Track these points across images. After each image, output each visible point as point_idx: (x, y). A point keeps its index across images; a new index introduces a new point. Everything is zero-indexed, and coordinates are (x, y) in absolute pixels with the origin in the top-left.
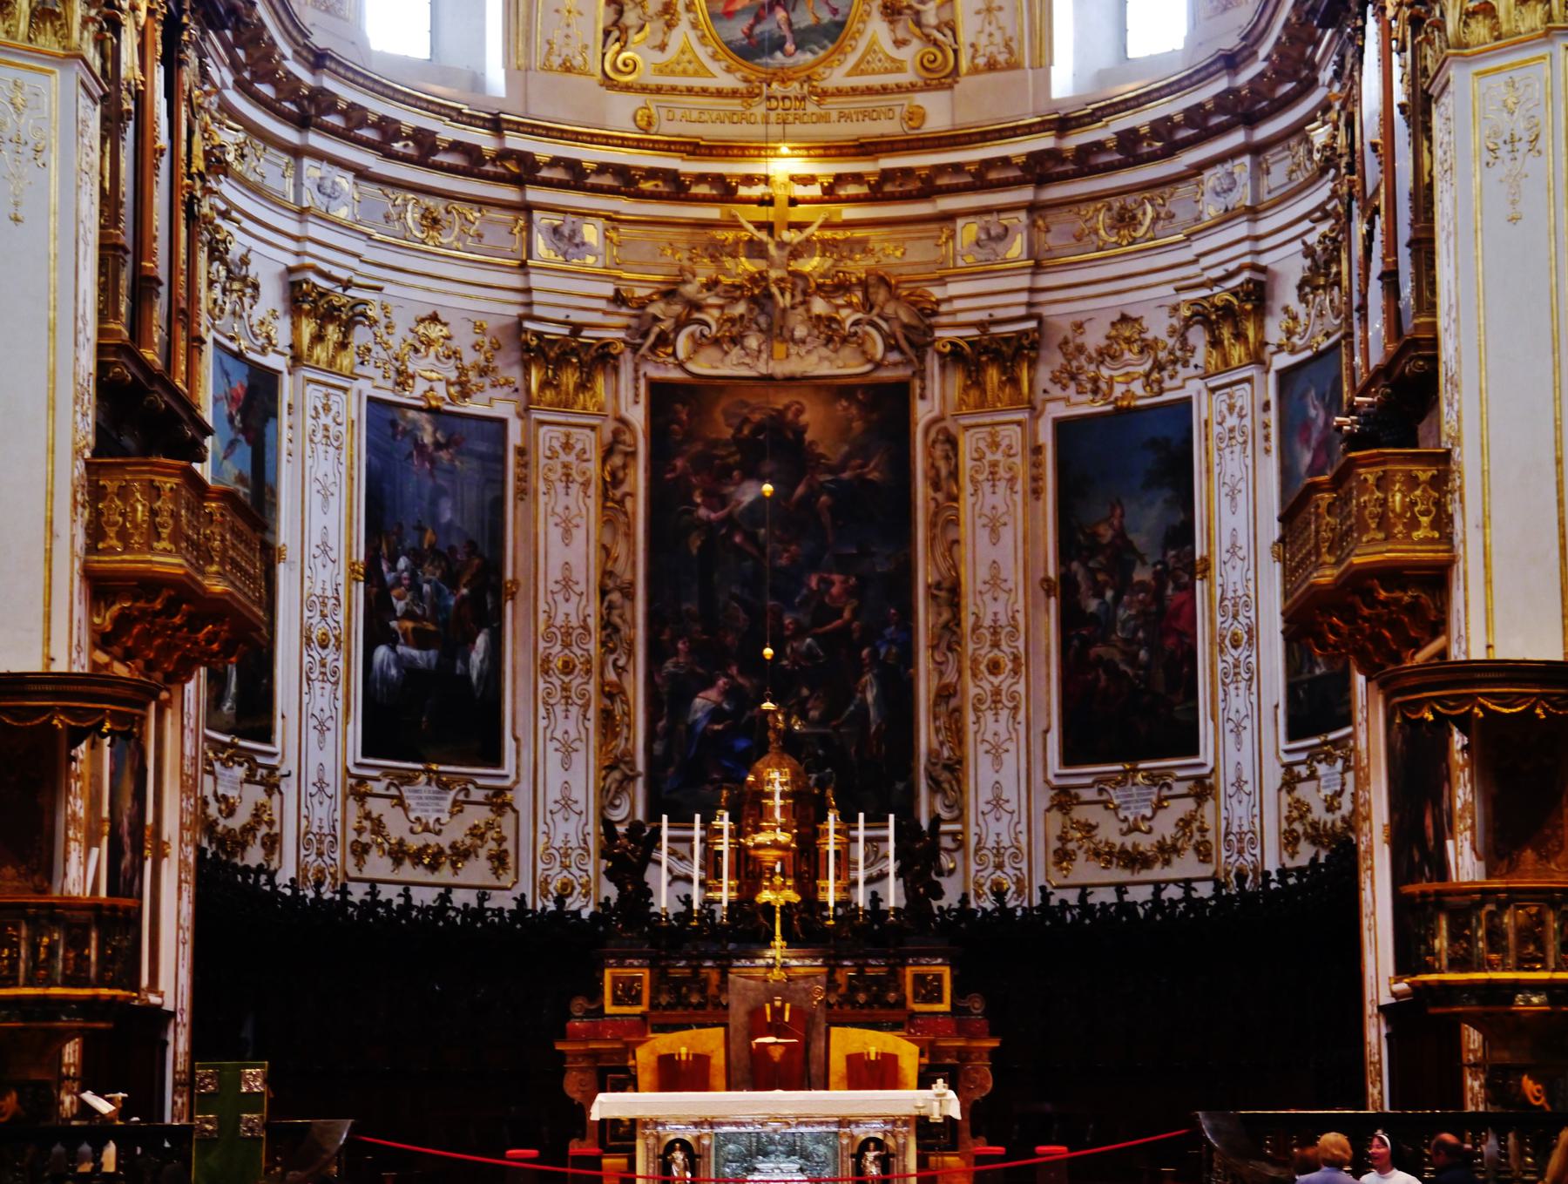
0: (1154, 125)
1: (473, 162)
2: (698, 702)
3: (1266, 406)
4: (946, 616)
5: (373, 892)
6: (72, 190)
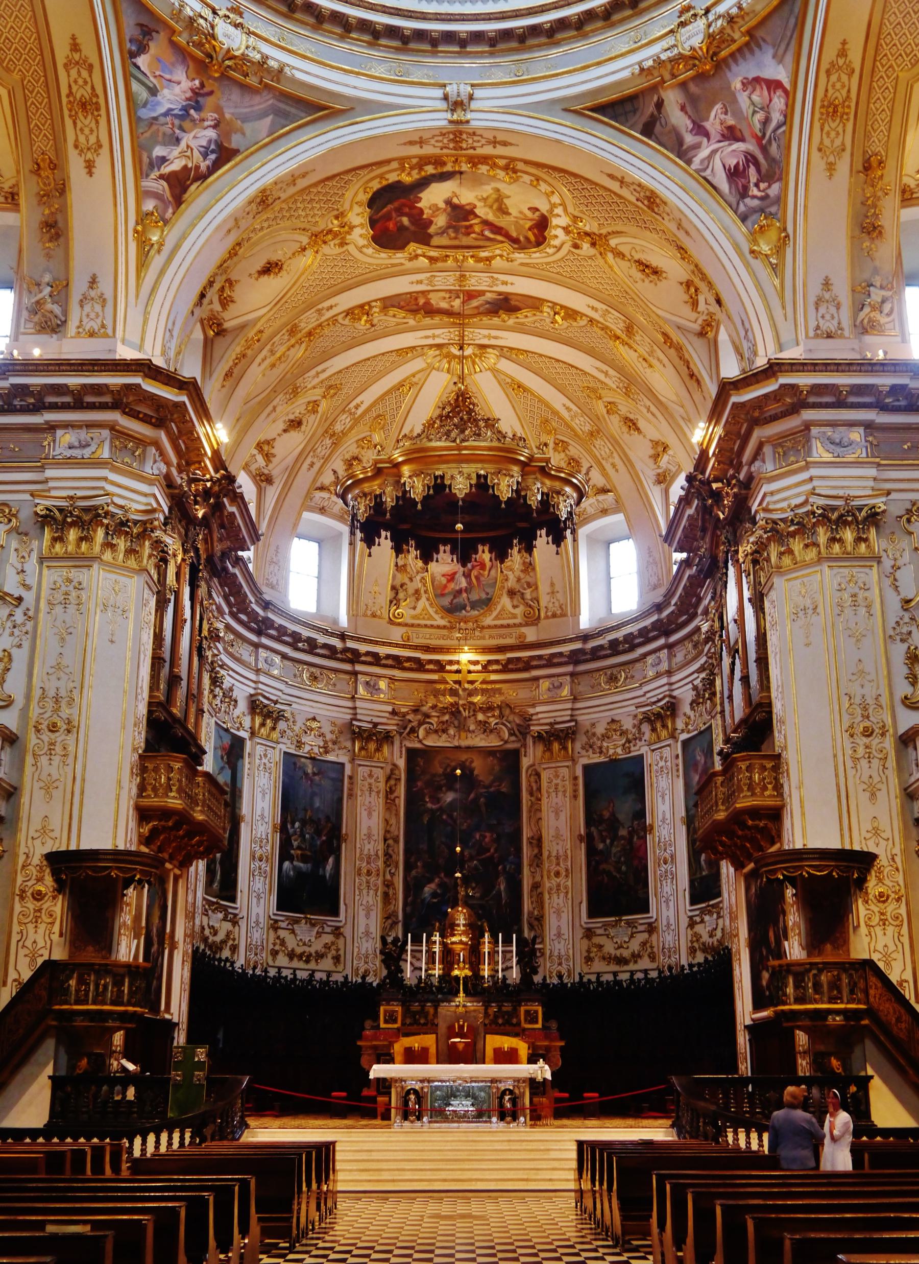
0: (625, 636)
1: (332, 653)
2: (426, 889)
3: (677, 756)
4: (536, 851)
5: (279, 972)
6: (139, 629)
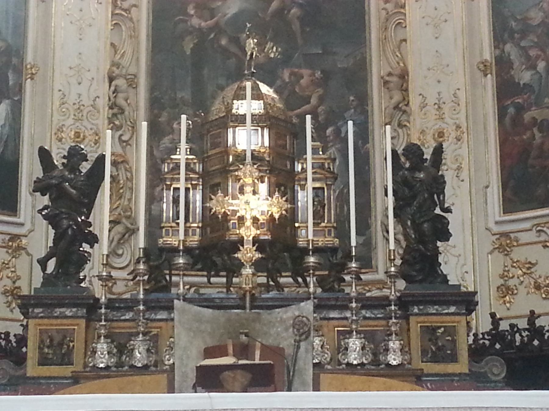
4: (397, 97)
